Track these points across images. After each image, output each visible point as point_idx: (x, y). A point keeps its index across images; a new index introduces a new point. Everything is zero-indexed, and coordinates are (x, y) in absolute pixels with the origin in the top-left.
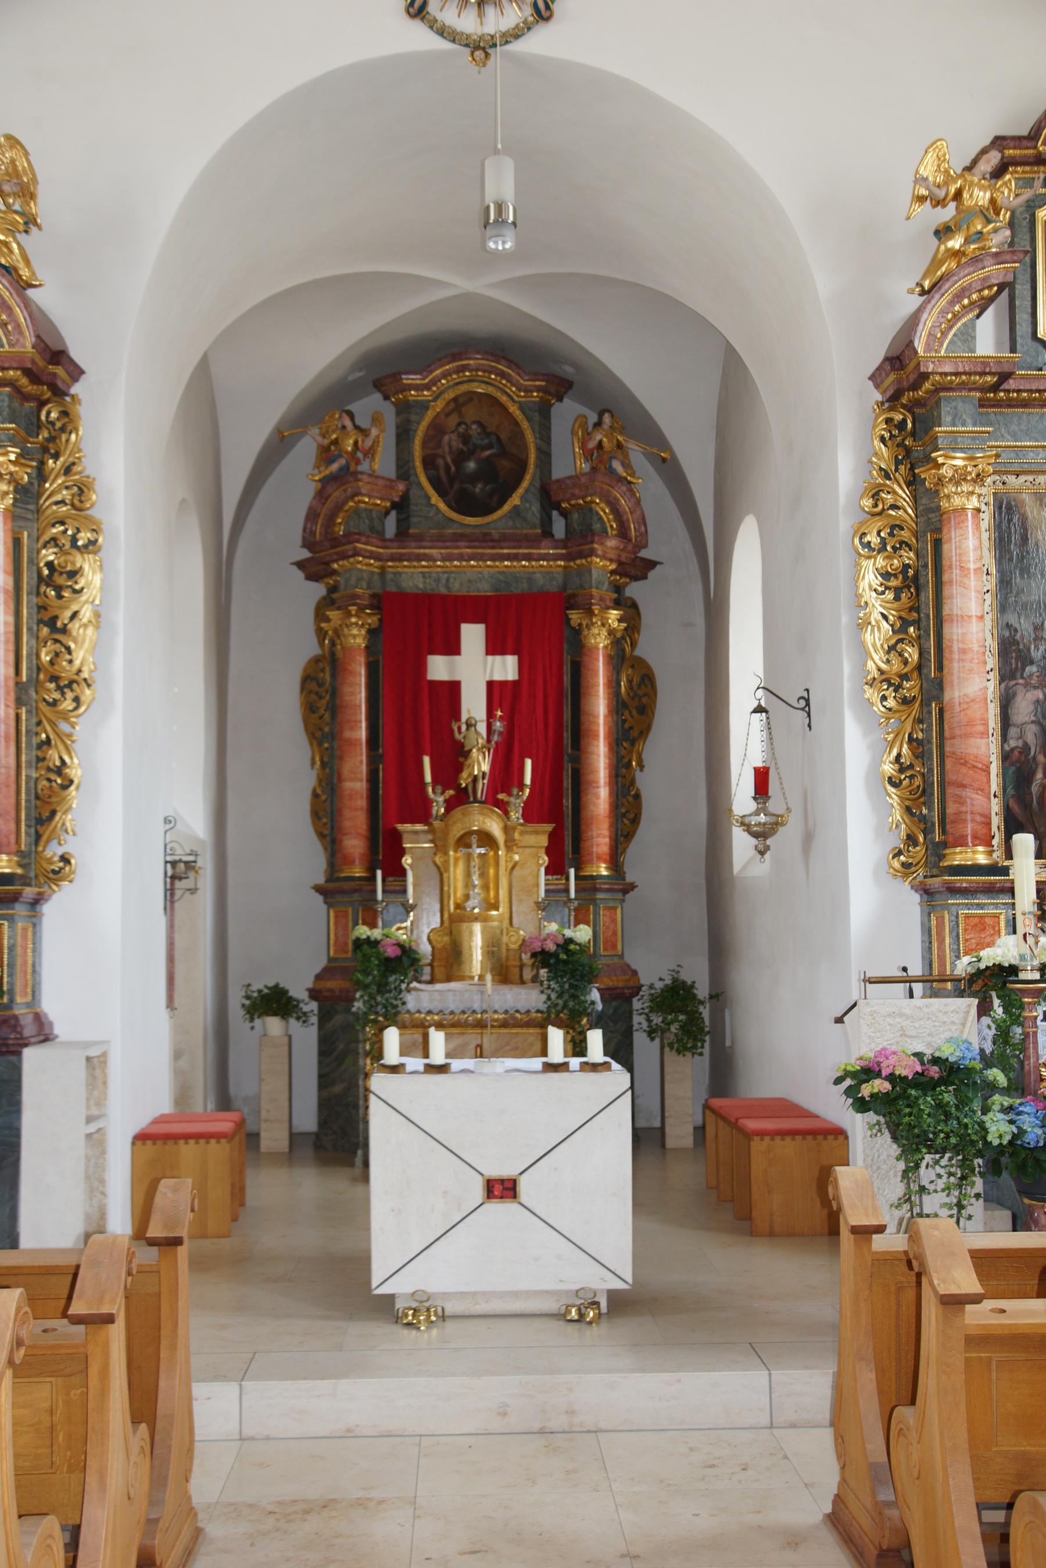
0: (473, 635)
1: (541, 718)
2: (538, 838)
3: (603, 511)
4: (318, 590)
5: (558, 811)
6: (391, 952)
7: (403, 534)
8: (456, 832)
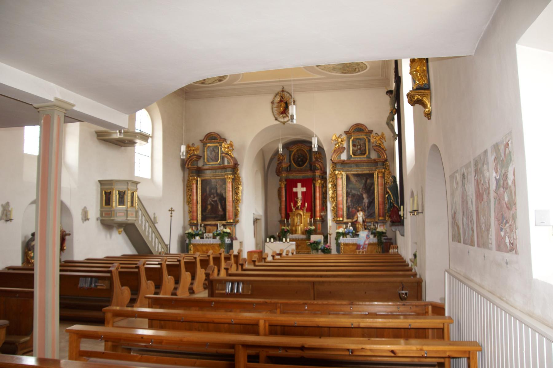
0: (299, 185)
1: (309, 197)
2: (309, 214)
3: (318, 166)
4: (279, 178)
5: (311, 210)
6: (286, 230)
7: (290, 170)
8: (296, 213)
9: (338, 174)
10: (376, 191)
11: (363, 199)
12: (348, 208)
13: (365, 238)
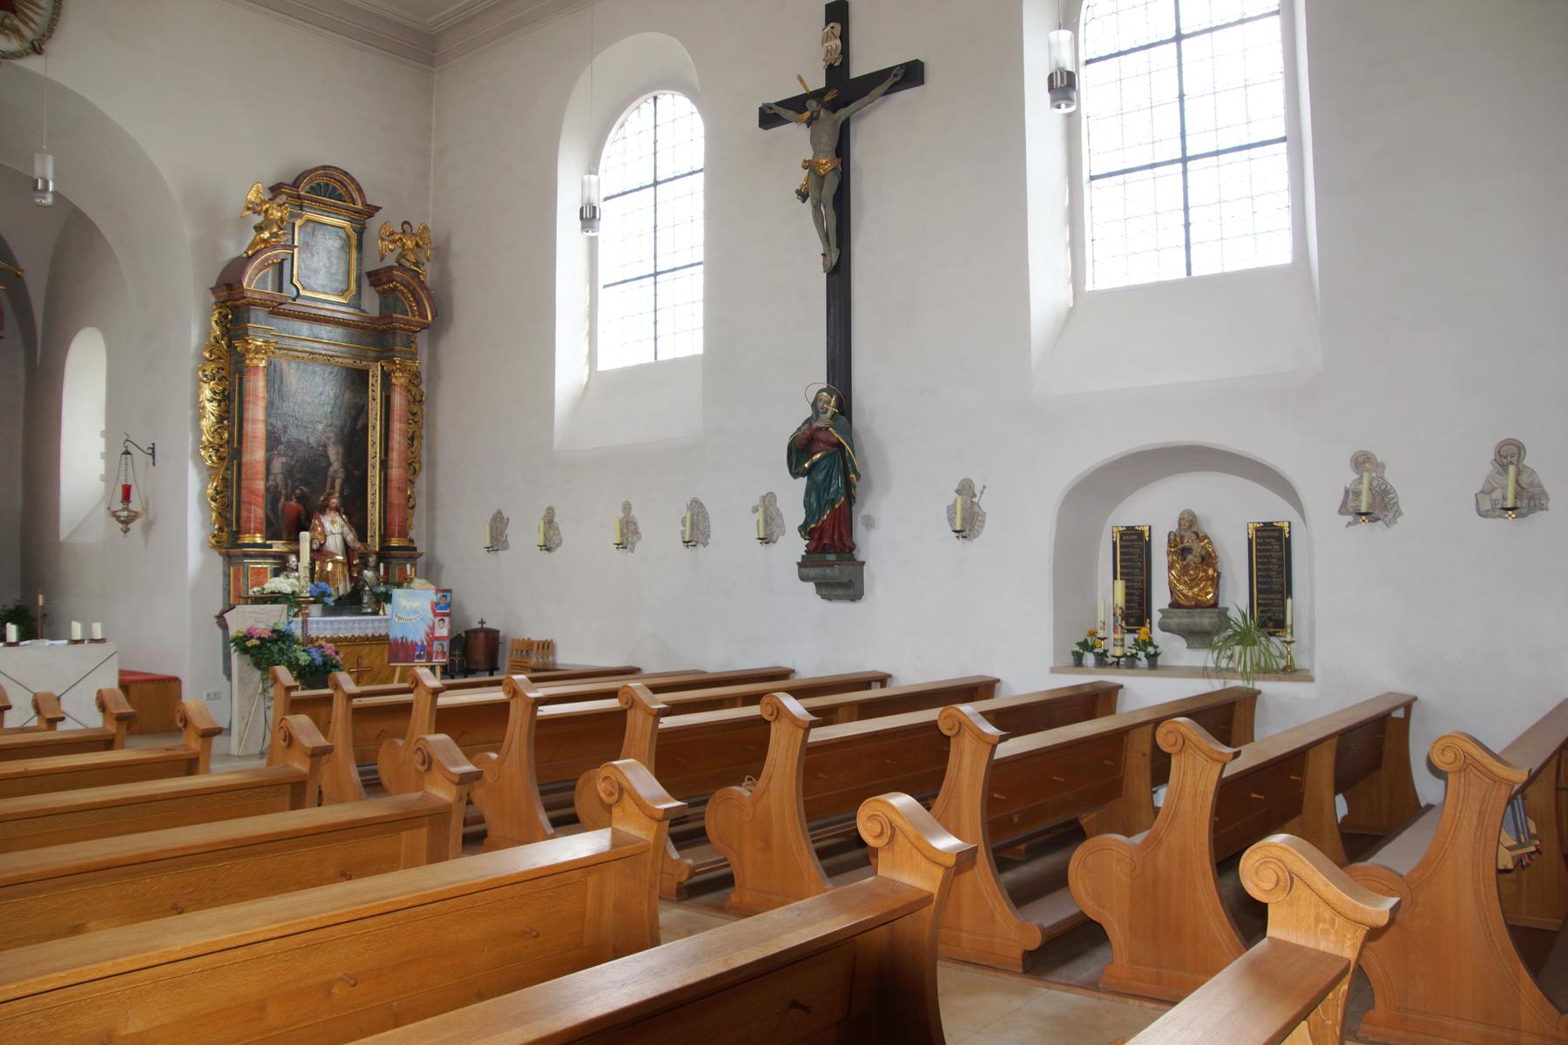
9: (257, 350)
10: (375, 436)
11: (330, 464)
12: (273, 496)
13: (431, 615)
